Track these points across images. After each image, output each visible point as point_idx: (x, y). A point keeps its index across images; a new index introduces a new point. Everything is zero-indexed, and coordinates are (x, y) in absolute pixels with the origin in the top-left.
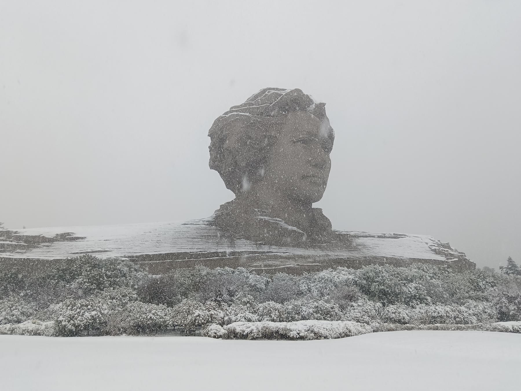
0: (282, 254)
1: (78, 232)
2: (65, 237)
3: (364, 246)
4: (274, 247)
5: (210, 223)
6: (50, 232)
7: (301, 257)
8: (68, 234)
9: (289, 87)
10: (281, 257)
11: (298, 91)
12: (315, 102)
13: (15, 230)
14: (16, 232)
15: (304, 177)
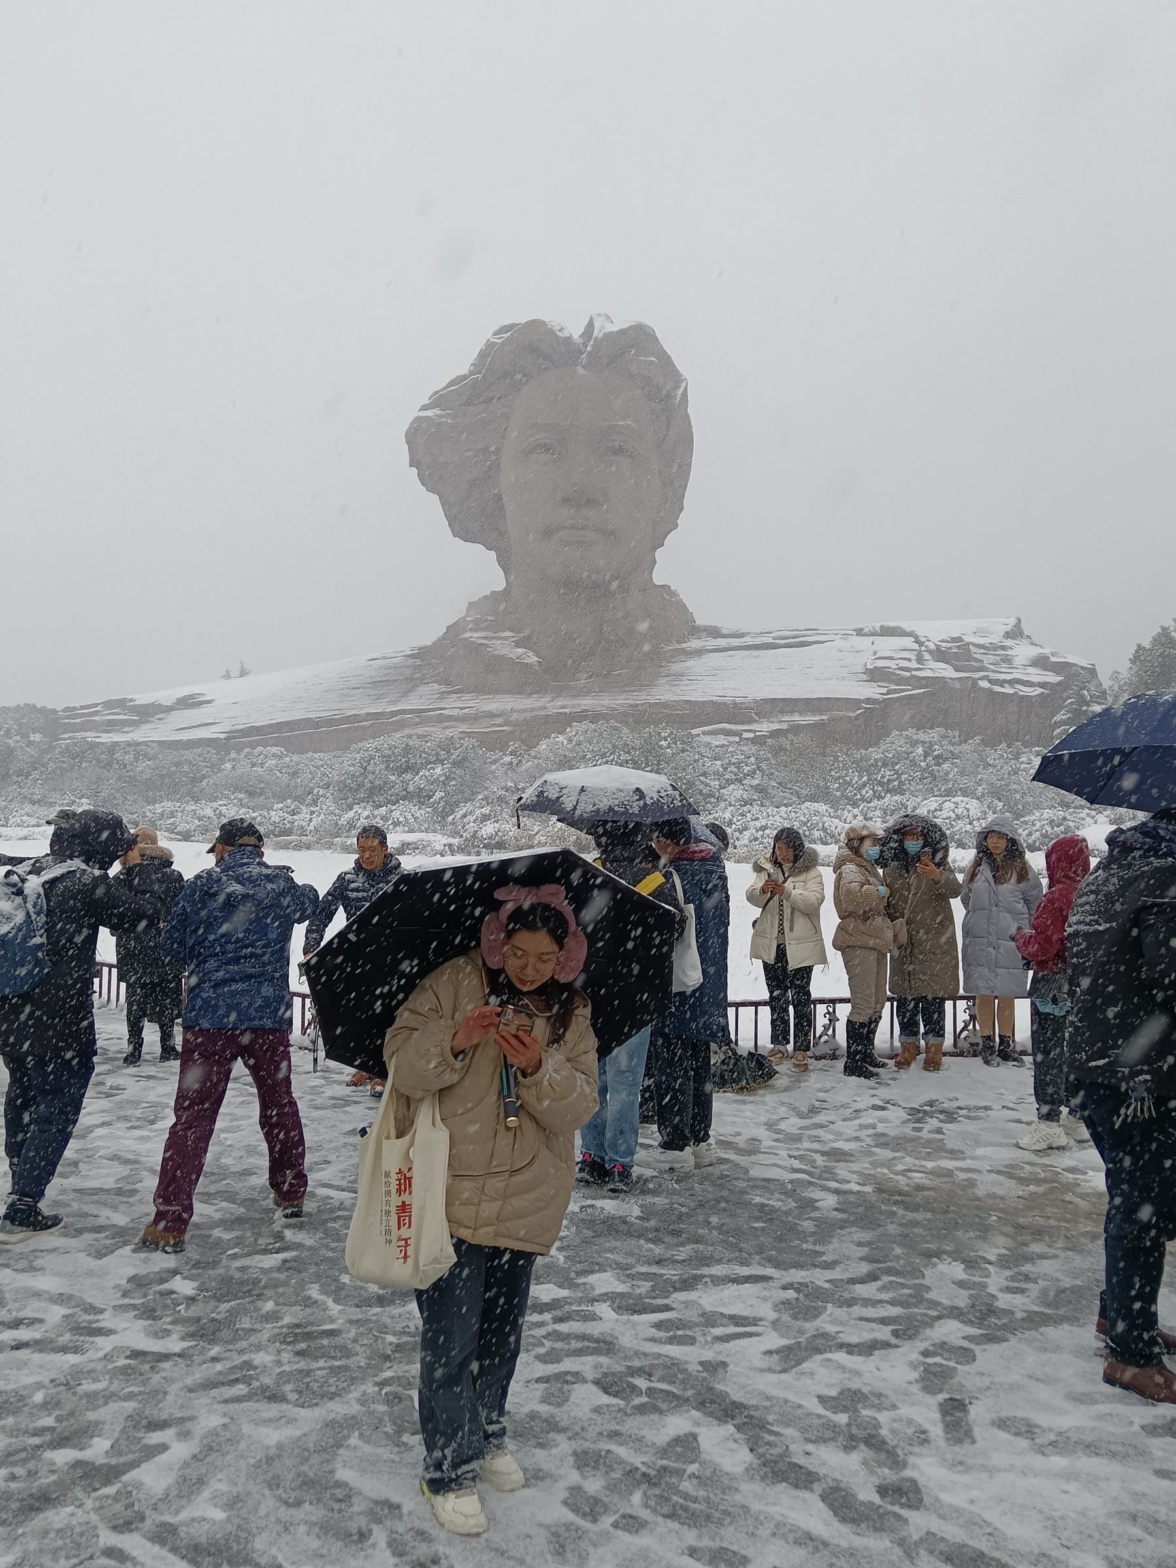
0: (456, 712)
1: (204, 689)
2: (189, 702)
3: (679, 676)
4: (468, 696)
5: (422, 654)
6: (167, 696)
7: (491, 715)
8: (192, 697)
9: (523, 320)
10: (450, 718)
11: (536, 325)
12: (596, 333)
13: (129, 697)
14: (131, 700)
15: (548, 533)
